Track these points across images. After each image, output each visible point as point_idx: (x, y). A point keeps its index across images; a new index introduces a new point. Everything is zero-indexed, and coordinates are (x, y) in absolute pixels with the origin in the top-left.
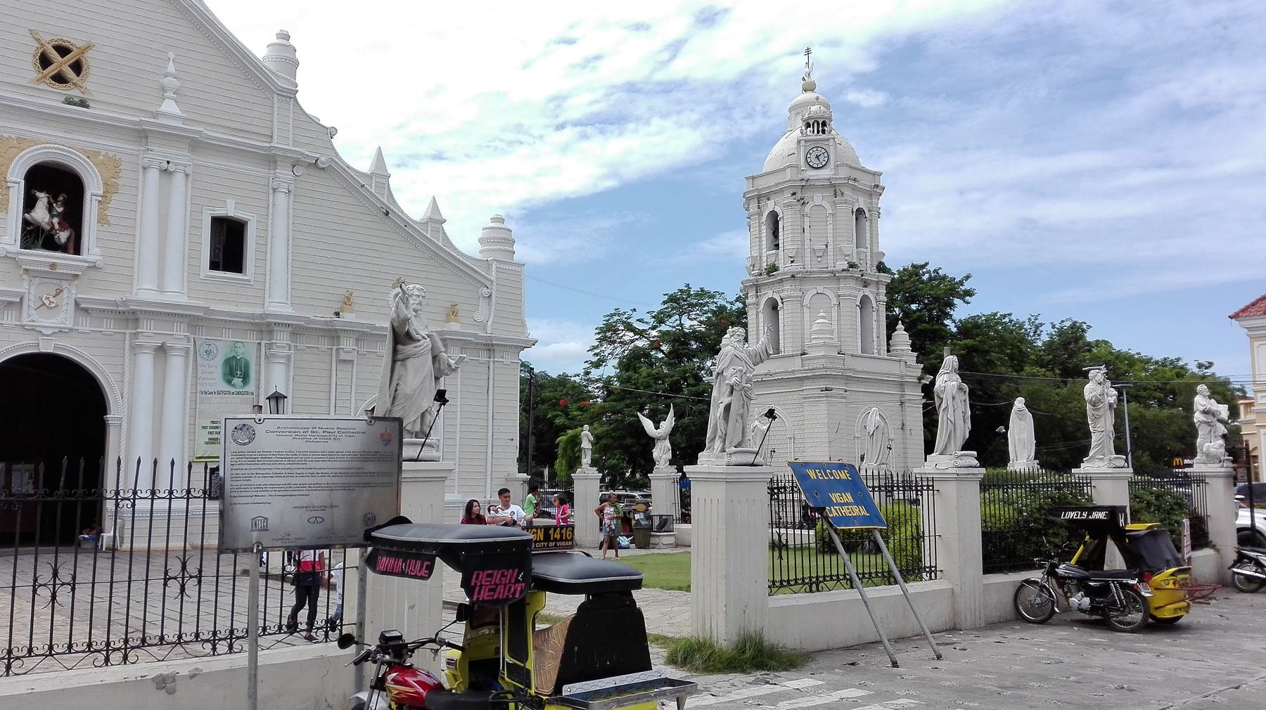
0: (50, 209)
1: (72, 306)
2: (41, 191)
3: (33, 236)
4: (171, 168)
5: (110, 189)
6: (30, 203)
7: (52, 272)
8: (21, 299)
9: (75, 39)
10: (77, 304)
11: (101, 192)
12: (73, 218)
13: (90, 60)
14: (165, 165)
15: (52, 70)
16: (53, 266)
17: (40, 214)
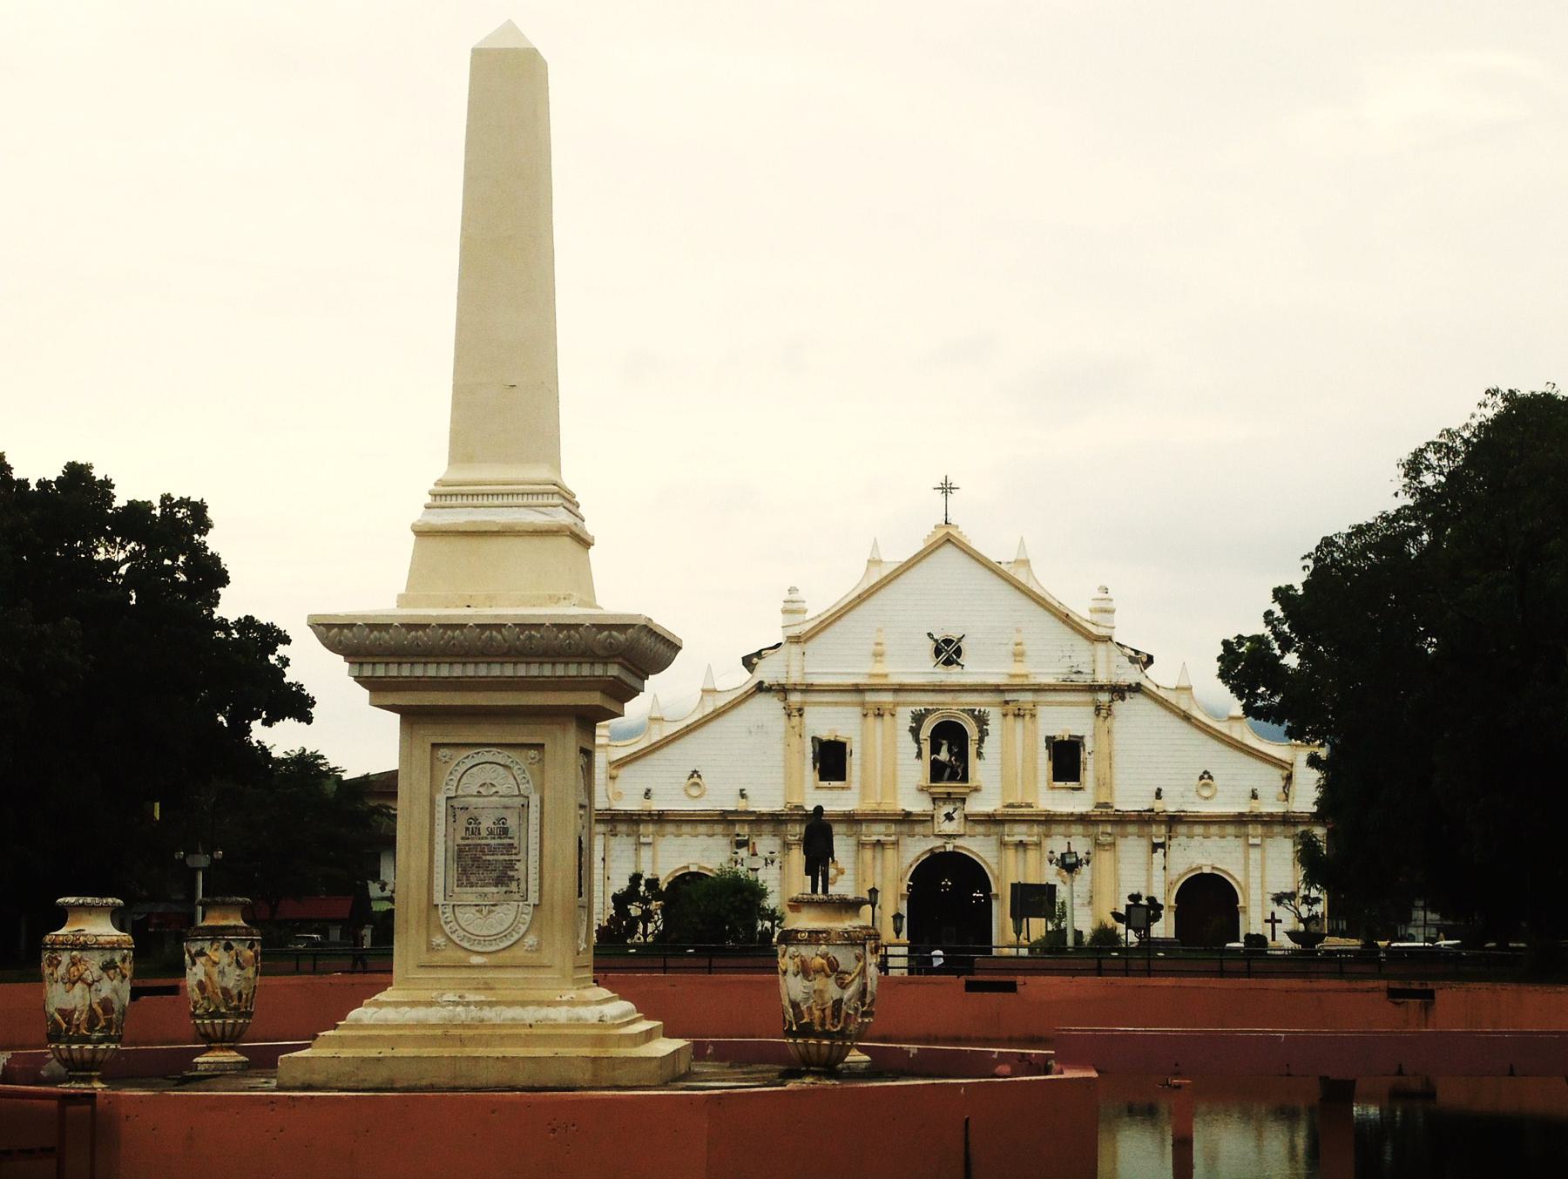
0: (950, 751)
1: (962, 820)
2: (944, 739)
3: (938, 771)
4: (1022, 712)
5: (983, 734)
6: (935, 749)
7: (948, 798)
8: (932, 816)
9: (955, 635)
10: (966, 816)
11: (978, 738)
12: (962, 756)
13: (963, 645)
14: (1016, 712)
15: (943, 656)
16: (949, 794)
17: (944, 756)
